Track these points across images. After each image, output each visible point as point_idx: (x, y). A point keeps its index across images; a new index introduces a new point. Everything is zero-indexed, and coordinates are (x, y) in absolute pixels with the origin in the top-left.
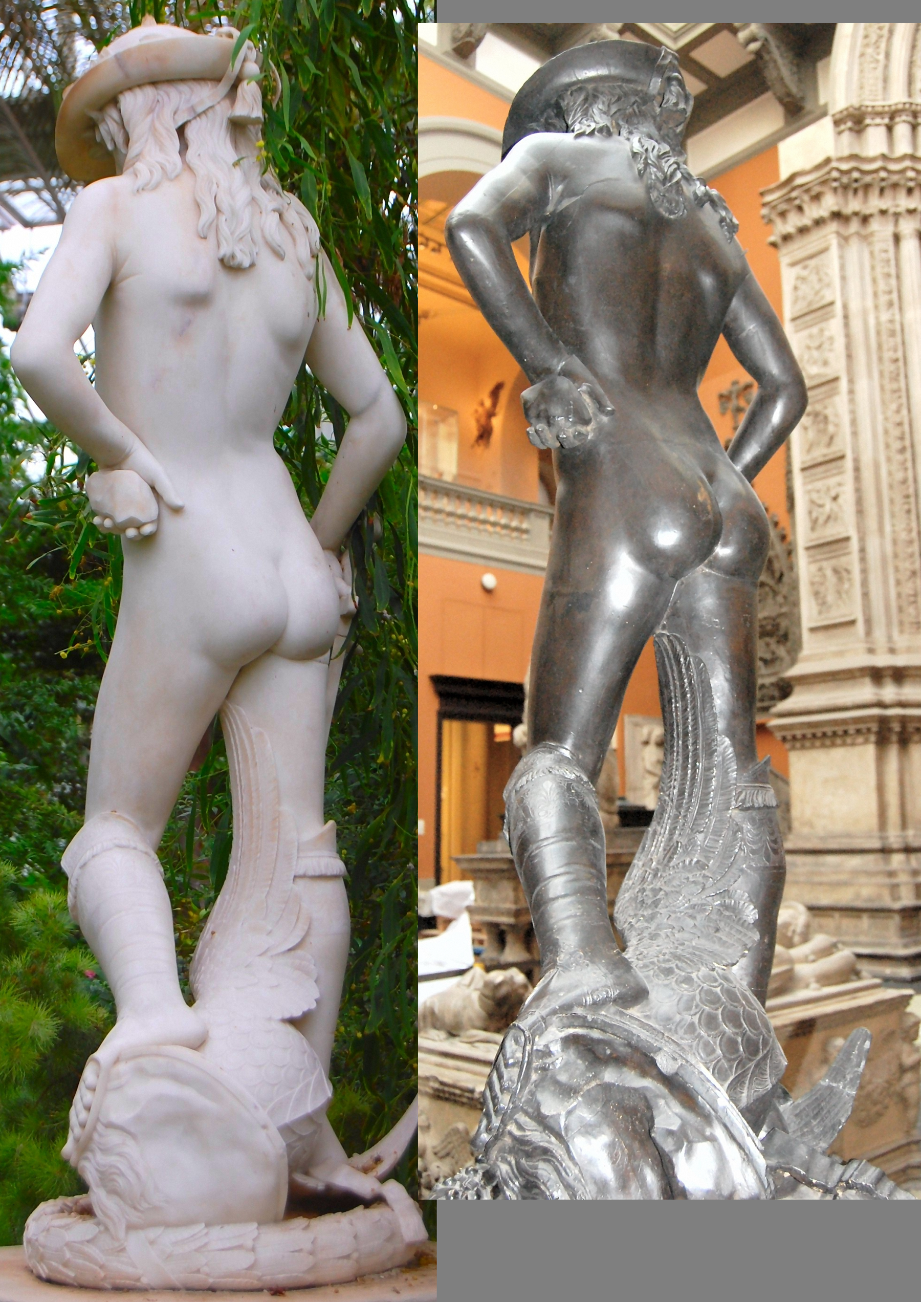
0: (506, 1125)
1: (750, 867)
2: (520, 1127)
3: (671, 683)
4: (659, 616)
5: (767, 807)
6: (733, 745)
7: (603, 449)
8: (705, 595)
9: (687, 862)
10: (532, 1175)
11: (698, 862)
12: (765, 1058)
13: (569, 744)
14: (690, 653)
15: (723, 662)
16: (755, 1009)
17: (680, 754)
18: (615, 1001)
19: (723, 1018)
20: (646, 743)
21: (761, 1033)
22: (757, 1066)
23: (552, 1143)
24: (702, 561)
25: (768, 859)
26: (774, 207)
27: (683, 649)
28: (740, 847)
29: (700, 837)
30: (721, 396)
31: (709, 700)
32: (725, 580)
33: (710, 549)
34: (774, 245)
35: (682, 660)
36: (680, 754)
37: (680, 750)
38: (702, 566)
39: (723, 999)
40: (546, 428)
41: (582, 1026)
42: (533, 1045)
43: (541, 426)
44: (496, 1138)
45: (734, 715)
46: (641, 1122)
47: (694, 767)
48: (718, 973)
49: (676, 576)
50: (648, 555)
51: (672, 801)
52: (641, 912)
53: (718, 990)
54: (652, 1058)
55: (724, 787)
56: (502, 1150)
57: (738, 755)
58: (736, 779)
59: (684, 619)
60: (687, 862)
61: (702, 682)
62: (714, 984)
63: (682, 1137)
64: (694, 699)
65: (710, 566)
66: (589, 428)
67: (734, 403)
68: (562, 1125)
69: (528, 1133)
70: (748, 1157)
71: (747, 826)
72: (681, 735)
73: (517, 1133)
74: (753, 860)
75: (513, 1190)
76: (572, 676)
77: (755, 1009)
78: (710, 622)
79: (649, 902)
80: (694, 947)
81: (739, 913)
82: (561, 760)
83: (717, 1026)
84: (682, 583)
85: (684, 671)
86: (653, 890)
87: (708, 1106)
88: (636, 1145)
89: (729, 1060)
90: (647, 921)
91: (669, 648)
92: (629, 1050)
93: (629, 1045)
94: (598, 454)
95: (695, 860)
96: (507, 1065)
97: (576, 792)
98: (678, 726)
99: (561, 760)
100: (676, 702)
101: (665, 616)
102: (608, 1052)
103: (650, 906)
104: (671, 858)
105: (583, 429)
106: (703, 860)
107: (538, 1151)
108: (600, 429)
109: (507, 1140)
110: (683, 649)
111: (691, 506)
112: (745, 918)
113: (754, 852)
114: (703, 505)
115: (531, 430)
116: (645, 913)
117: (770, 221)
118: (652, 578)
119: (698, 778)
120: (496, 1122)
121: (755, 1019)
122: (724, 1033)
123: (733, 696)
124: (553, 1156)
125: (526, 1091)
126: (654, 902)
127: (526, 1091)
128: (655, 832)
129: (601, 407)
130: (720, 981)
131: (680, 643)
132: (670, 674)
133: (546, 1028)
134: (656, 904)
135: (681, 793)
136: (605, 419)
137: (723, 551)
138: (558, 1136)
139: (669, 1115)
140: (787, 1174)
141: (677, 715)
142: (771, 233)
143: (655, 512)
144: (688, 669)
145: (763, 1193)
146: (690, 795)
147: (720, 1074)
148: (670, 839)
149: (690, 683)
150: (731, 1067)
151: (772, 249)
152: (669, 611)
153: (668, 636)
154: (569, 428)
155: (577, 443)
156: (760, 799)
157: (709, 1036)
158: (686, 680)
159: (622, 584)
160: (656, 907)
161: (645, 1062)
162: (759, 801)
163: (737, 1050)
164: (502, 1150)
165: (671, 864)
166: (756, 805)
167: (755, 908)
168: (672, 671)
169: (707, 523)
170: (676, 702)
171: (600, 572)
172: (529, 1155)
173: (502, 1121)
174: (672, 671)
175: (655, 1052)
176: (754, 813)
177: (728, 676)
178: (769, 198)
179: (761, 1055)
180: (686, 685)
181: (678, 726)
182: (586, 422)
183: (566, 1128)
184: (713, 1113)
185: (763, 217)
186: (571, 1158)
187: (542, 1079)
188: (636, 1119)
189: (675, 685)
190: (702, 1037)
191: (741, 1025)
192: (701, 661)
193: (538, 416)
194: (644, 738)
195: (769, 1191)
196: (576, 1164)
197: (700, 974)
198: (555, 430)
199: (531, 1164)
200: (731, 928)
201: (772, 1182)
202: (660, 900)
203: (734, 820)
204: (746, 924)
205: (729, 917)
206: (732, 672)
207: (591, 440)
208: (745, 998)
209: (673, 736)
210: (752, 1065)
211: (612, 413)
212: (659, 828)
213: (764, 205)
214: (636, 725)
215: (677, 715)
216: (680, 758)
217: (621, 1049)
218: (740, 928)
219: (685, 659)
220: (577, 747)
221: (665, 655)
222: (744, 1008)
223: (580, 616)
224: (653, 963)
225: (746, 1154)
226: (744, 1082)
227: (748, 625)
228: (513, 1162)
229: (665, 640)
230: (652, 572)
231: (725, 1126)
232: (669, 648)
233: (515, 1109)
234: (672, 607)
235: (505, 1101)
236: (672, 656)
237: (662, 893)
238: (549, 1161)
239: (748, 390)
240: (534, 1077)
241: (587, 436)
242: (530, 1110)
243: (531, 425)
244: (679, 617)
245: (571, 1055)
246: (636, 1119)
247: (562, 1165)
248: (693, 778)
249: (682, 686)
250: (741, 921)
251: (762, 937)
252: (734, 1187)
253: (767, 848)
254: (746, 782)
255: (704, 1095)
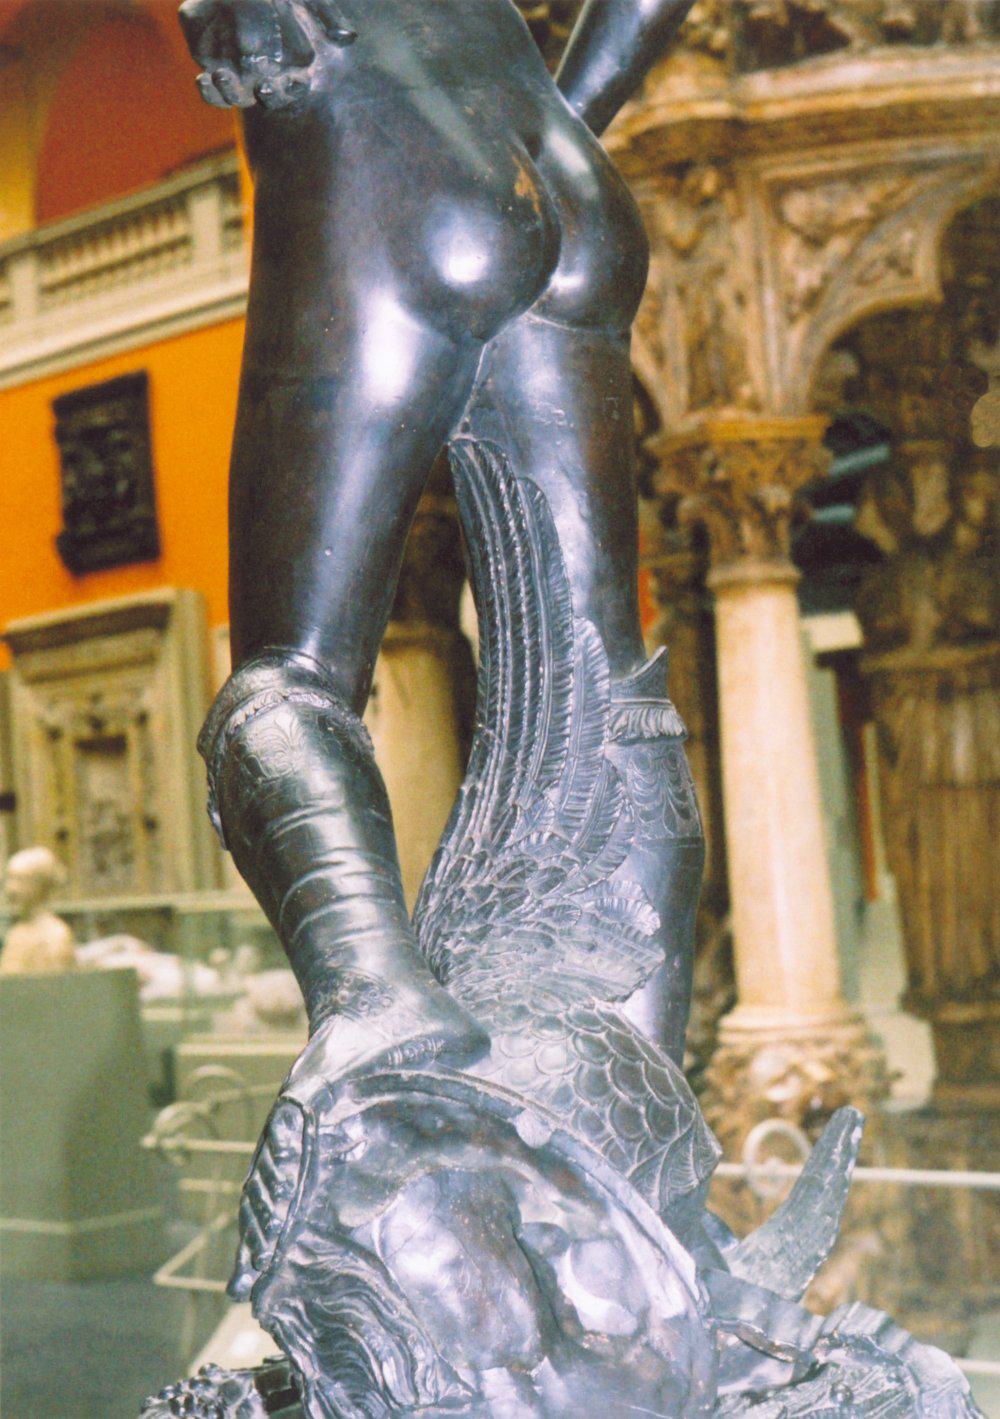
0: (284, 1252)
1: (644, 842)
2: (307, 1251)
3: (486, 529)
4: (457, 408)
5: (663, 736)
6: (602, 632)
7: (339, 108)
8: (537, 366)
9: (534, 838)
10: (335, 1319)
11: (552, 836)
12: (684, 1139)
13: (310, 646)
14: (516, 474)
15: (575, 487)
16: (664, 1066)
17: (510, 653)
18: (438, 1056)
19: (614, 1077)
21: (677, 1102)
22: (674, 1149)
23: (363, 1270)
24: (527, 305)
25: (673, 827)
27: (504, 468)
28: (623, 808)
29: (553, 795)
31: (553, 554)
32: (571, 335)
33: (543, 280)
35: (502, 486)
36: (510, 653)
37: (510, 648)
38: (527, 313)
39: (612, 1050)
40: (233, 75)
41: (390, 1091)
42: (317, 1127)
43: (226, 72)
44: (270, 1274)
45: (599, 579)
46: (500, 1226)
47: (536, 677)
48: (599, 1011)
49: (484, 336)
50: (433, 301)
51: (500, 736)
52: (459, 929)
53: (602, 1036)
54: (510, 1124)
55: (593, 707)
56: (280, 1293)
57: (611, 650)
58: (609, 692)
59: (502, 414)
60: (534, 838)
61: (541, 524)
62: (595, 1028)
63: (564, 1240)
64: (527, 556)
65: (544, 310)
66: (311, 70)
68: (376, 1238)
69: (320, 1259)
70: (666, 1258)
71: (633, 772)
72: (509, 622)
73: (303, 1260)
74: (646, 829)
75: (304, 1350)
76: (307, 529)
77: (664, 1066)
78: (551, 415)
79: (474, 910)
80: (556, 975)
81: (629, 918)
82: (299, 678)
83: (606, 1089)
84: (495, 346)
85: (507, 506)
86: (478, 889)
87: (601, 1187)
88: (494, 1260)
89: (628, 1140)
90: (472, 941)
91: (477, 465)
92: (472, 1117)
93: (473, 1109)
94: (331, 118)
95: (546, 835)
96: (278, 1161)
97: (336, 729)
98: (502, 605)
99: (299, 678)
100: (497, 562)
101: (467, 408)
102: (440, 1124)
103: (476, 917)
104: (505, 836)
105: (295, 74)
106: (561, 834)
107: (340, 1283)
108: (331, 71)
109: (288, 1277)
110: (504, 468)
111: (505, 209)
112: (638, 927)
113: (646, 816)
114: (526, 204)
115: (205, 77)
116: (468, 929)
118: (443, 341)
119: (543, 694)
120: (268, 1249)
121: (666, 1081)
122: (617, 1099)
123: (596, 547)
124: (365, 1285)
125: (313, 1197)
126: (482, 910)
127: (313, 1197)
128: (473, 792)
129: (330, 32)
130: (604, 1023)
131: (498, 457)
132: (482, 514)
133: (335, 1100)
134: (486, 911)
135: (516, 720)
136: (338, 52)
137: (566, 282)
138: (368, 1255)
139: (542, 1205)
140: (733, 1340)
141: (499, 586)
143: (441, 222)
144: (514, 502)
145: (693, 1308)
146: (532, 722)
147: (618, 1160)
148: (501, 802)
149: (519, 528)
150: (630, 1152)
152: (472, 399)
153: (475, 445)
154: (276, 75)
155: (290, 98)
156: (652, 723)
157: (592, 1104)
158: (512, 523)
159: (386, 353)
160: (486, 917)
161: (496, 1129)
162: (650, 728)
163: (639, 1127)
164: (280, 1293)
165: (508, 843)
166: (647, 735)
167: (654, 909)
168: (486, 507)
169: (536, 233)
170: (497, 562)
171: (346, 334)
172: (324, 1291)
173: (279, 1246)
174: (486, 507)
175: (514, 1116)
176: (644, 749)
177: (585, 510)
179: (678, 1135)
180: (513, 530)
181: (502, 605)
182: (303, 59)
183: (383, 1243)
184: (609, 1196)
186: (394, 1288)
187: (338, 1176)
188: (492, 1221)
189: (492, 532)
190: (582, 1106)
191: (643, 1089)
192: (535, 488)
193: (217, 55)
195: (701, 1304)
196: (402, 1296)
197: (571, 1012)
198: (250, 81)
199: (330, 1303)
200: (617, 944)
201: (705, 1291)
202: (492, 905)
203: (608, 762)
204: (641, 938)
205: (609, 927)
206: (591, 504)
207: (315, 92)
208: (649, 1050)
209: (493, 625)
210: (665, 1149)
211: (352, 37)
212: (480, 786)
215: (499, 586)
216: (510, 661)
217: (461, 1117)
218: (631, 944)
219: (509, 485)
220: (325, 651)
221: (470, 478)
222: (647, 1064)
223: (318, 420)
224: (491, 1001)
225: (663, 1253)
226: (652, 1176)
227: (616, 416)
228: (301, 1307)
229: (469, 451)
230: (441, 330)
231: (630, 1214)
232: (477, 465)
233: (298, 1226)
234: (479, 392)
235: (280, 1212)
236: (484, 483)
237: (494, 892)
238: (357, 1295)
240: (323, 1175)
241: (309, 85)
242: (322, 1224)
243: (203, 69)
244: (492, 408)
245: (380, 1133)
246: (492, 1221)
247: (379, 1298)
248: (535, 696)
249: (506, 532)
250: (633, 933)
251: (669, 958)
252: (648, 1301)
253: (669, 807)
254: (626, 695)
255: (593, 1171)
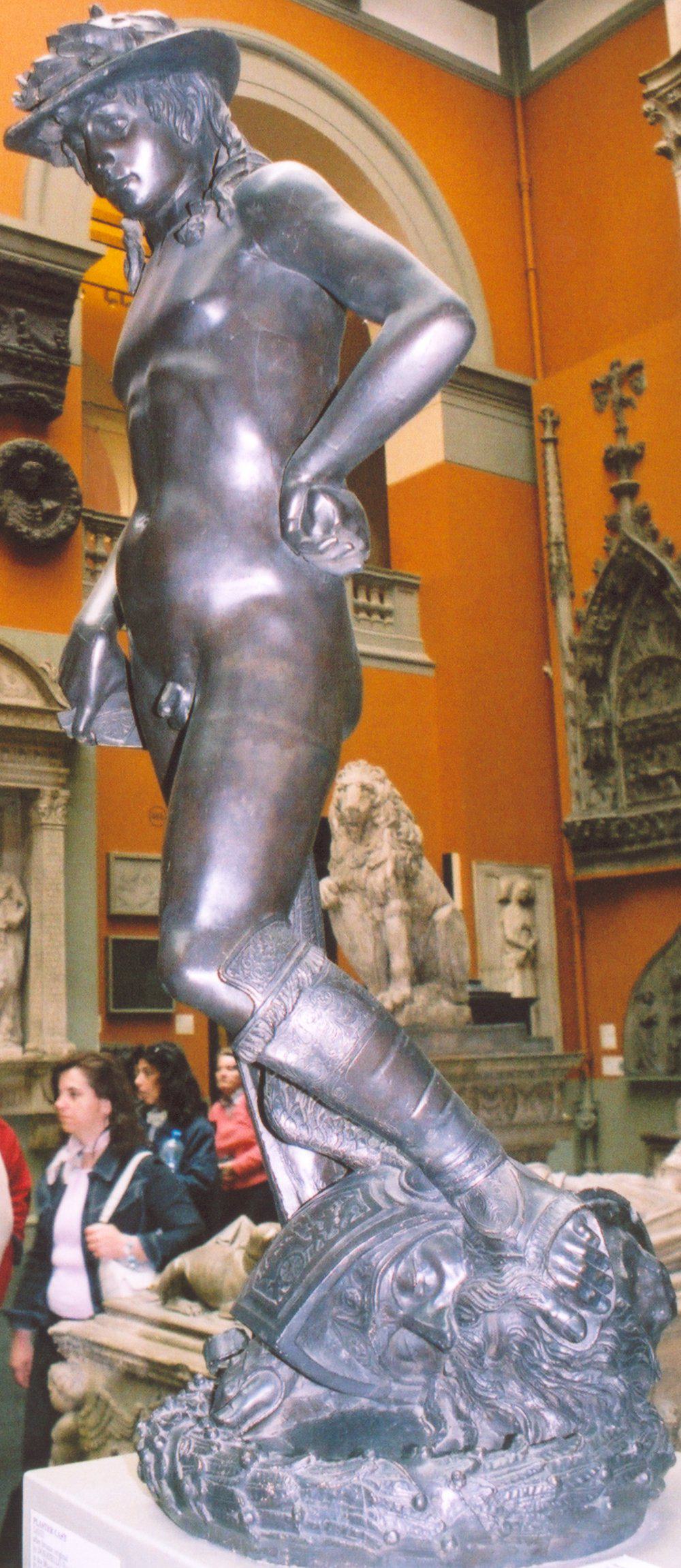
20: (505, 901)
26: (662, 99)
30: (595, 386)
34: (665, 153)
67: (616, 392)
117: (659, 119)
142: (660, 136)
151: (664, 159)
178: (653, 85)
185: (646, 114)
194: (502, 895)
213: (647, 96)
214: (490, 875)
239: (637, 374)
